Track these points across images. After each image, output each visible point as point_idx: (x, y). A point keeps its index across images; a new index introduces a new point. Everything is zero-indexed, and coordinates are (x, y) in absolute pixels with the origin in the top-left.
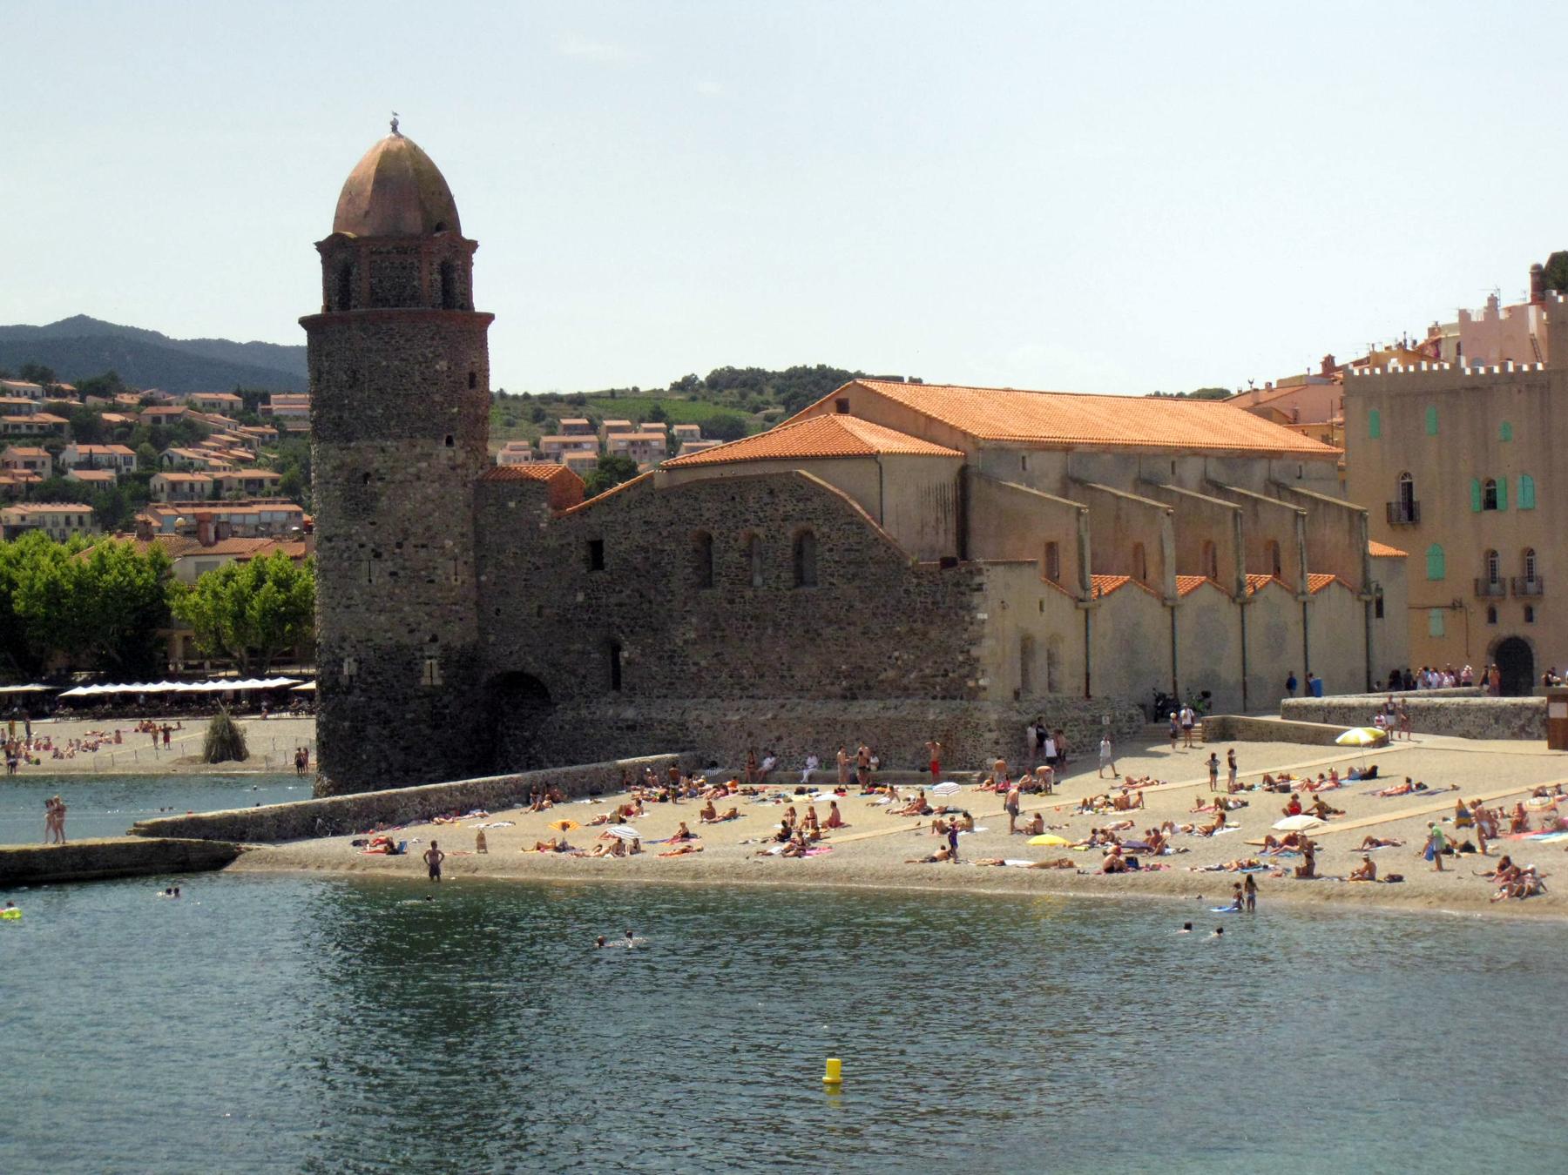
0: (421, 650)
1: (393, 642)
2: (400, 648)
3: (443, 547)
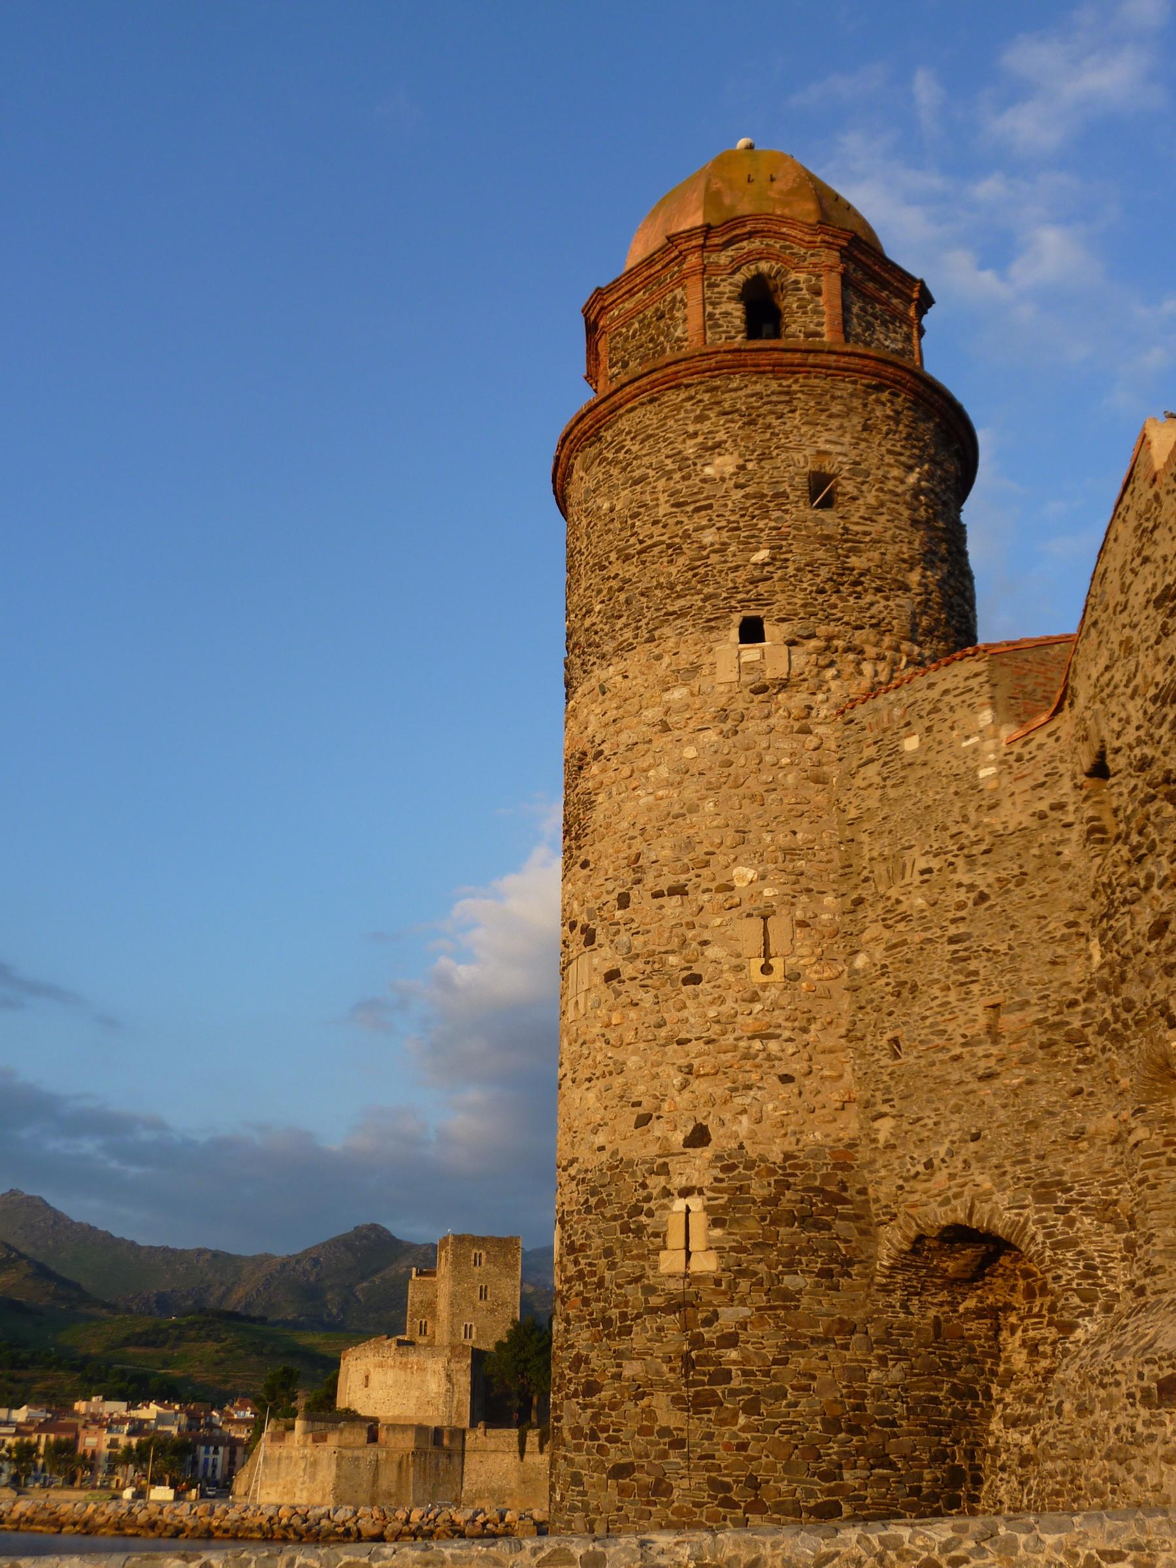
0: (664, 1170)
1: (604, 1156)
2: (619, 1166)
3: (728, 888)
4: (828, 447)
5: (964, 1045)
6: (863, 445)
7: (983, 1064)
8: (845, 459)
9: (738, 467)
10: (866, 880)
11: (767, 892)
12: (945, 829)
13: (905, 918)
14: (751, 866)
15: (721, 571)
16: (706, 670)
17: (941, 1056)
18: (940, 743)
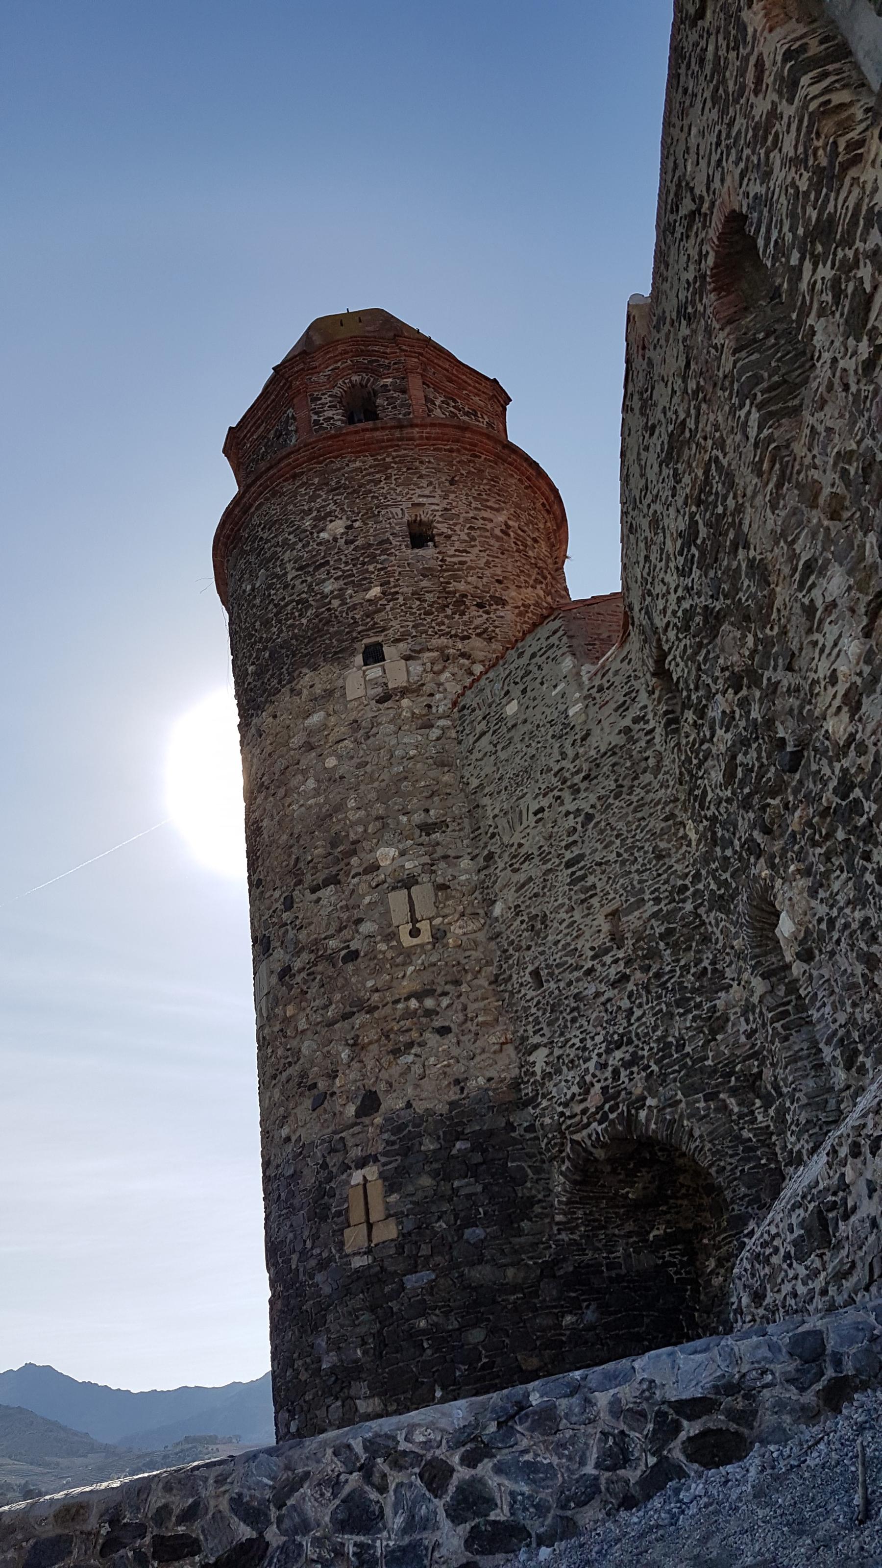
4: (421, 500)
5: (593, 958)
6: (452, 496)
7: (613, 971)
8: (437, 508)
9: (346, 528)
10: (493, 835)
11: (408, 865)
12: (550, 770)
13: (528, 857)
14: (389, 845)
15: (341, 612)
16: (337, 694)
17: (576, 974)
18: (535, 699)
